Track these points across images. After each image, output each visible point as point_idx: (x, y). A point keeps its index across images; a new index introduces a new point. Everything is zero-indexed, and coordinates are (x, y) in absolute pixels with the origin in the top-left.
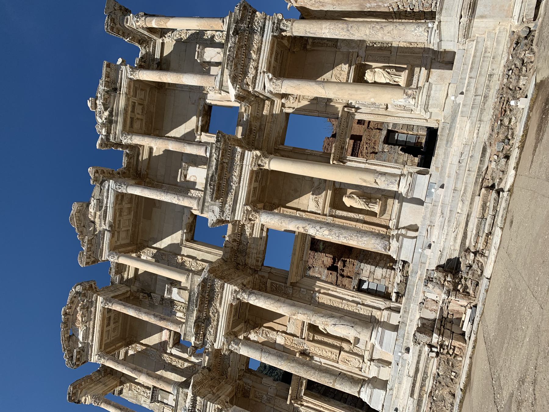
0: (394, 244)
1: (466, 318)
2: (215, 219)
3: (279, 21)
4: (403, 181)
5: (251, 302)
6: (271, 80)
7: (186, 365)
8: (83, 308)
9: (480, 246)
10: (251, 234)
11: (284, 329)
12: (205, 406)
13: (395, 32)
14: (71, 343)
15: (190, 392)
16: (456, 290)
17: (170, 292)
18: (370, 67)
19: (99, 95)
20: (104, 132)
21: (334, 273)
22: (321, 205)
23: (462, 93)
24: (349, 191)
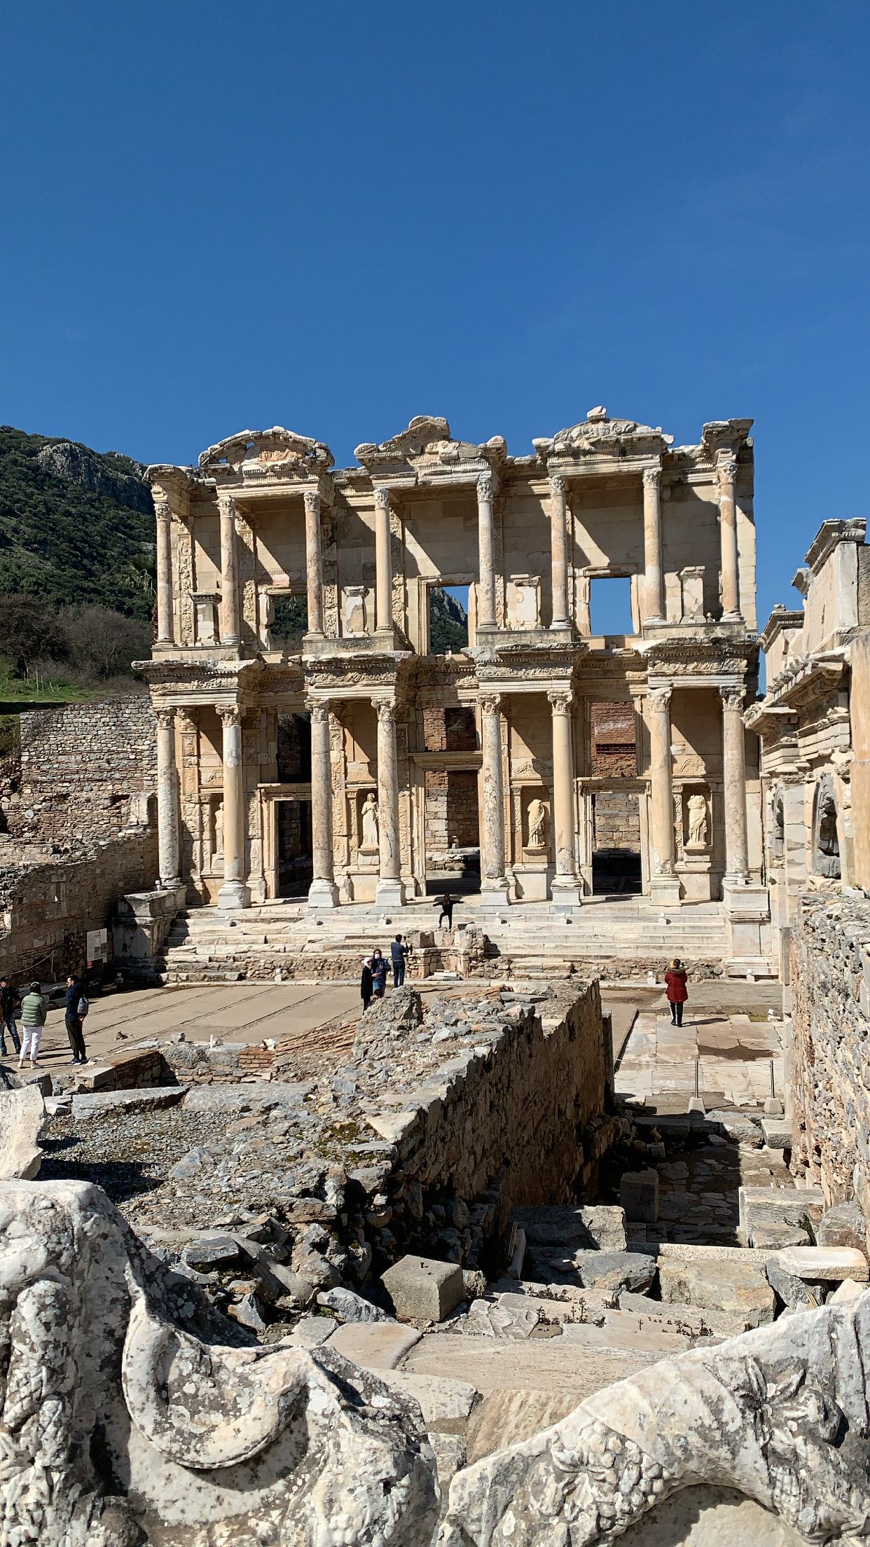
0: (497, 883)
1: (446, 973)
2: (472, 656)
3: (738, 693)
4: (569, 879)
5: (380, 725)
6: (663, 696)
7: (252, 624)
9: (517, 972)
10: (461, 687)
11: (350, 758)
13: (734, 837)
14: (234, 449)
15: (237, 665)
16: (471, 959)
18: (707, 799)
19: (611, 424)
20: (559, 447)
22: (522, 775)
23: (668, 922)
24: (547, 804)
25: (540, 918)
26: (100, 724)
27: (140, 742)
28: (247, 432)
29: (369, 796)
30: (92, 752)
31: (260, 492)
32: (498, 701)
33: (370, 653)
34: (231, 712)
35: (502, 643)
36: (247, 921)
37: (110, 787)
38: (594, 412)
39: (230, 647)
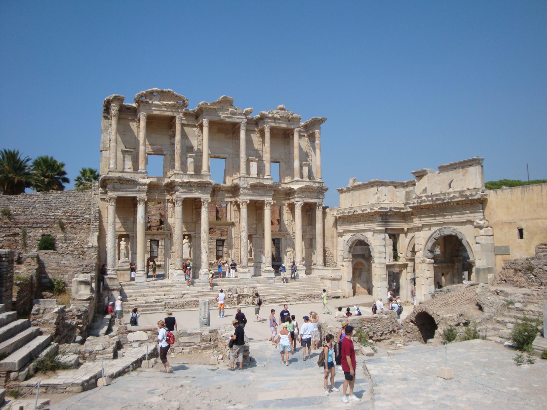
8: (175, 104)
12: (143, 191)
15: (147, 181)
17: (191, 157)
20: (270, 115)
21: (159, 224)
25: (264, 283)
26: (37, 202)
27: (57, 211)
28: (156, 89)
29: (186, 237)
30: (32, 215)
31: (159, 113)
32: (248, 202)
33: (204, 180)
34: (143, 200)
35: (252, 182)
36: (153, 287)
37: (41, 231)
38: (281, 106)
39: (143, 173)
